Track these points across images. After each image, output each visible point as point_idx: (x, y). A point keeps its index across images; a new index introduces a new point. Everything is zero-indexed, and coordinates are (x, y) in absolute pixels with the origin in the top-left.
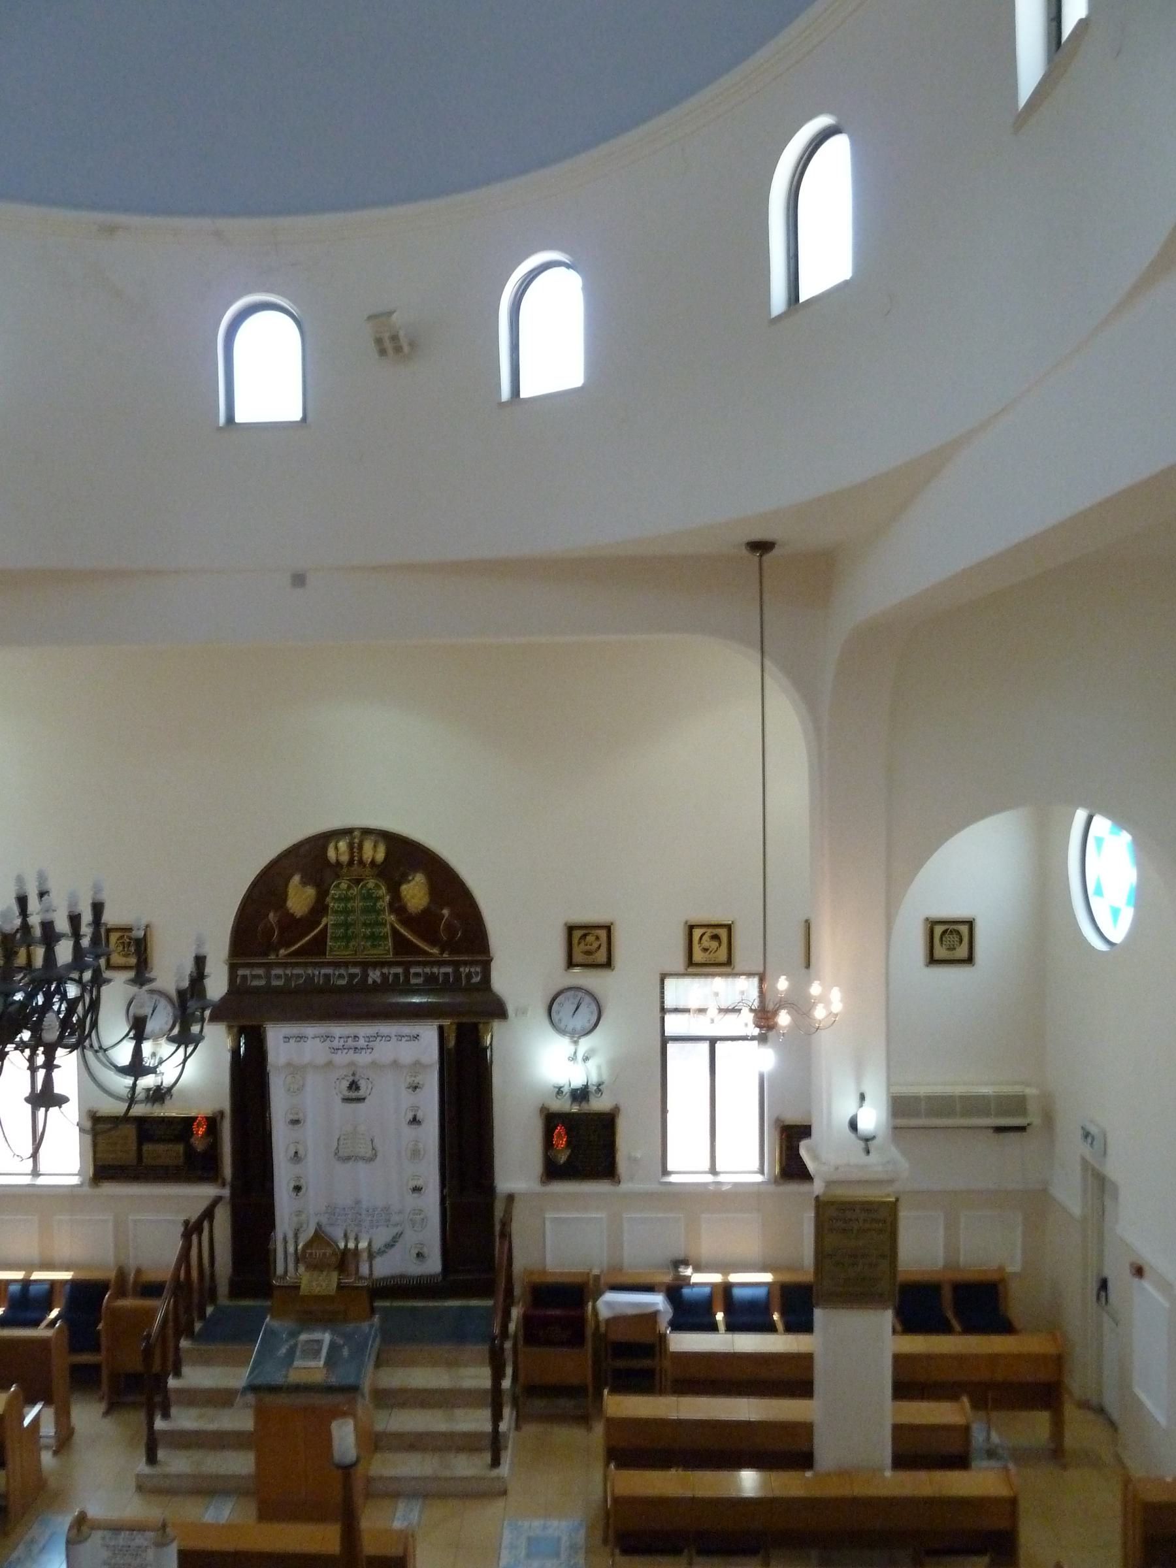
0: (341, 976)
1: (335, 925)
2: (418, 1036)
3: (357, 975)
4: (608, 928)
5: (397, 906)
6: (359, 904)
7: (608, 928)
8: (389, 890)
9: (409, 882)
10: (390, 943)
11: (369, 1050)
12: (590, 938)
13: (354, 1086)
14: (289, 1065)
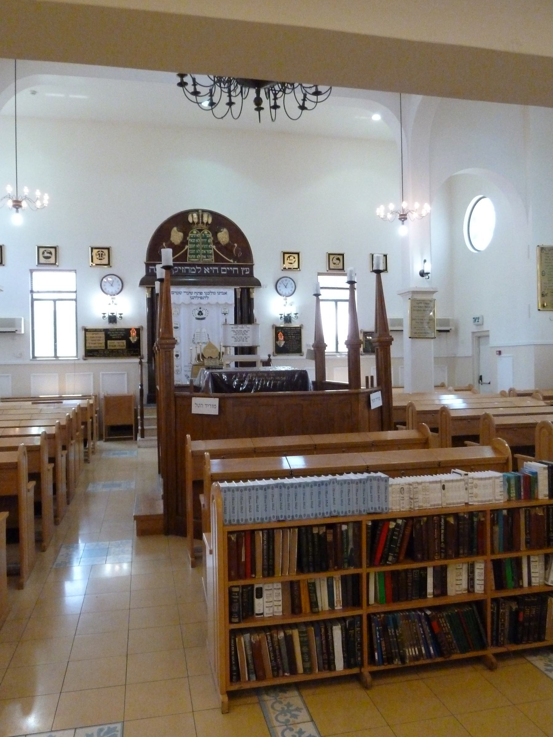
1: (190, 249)
3: (200, 269)
4: (298, 254)
5: (216, 242)
6: (200, 240)
7: (298, 254)
8: (212, 236)
9: (221, 231)
10: (213, 256)
11: (207, 298)
12: (291, 258)
13: (200, 313)
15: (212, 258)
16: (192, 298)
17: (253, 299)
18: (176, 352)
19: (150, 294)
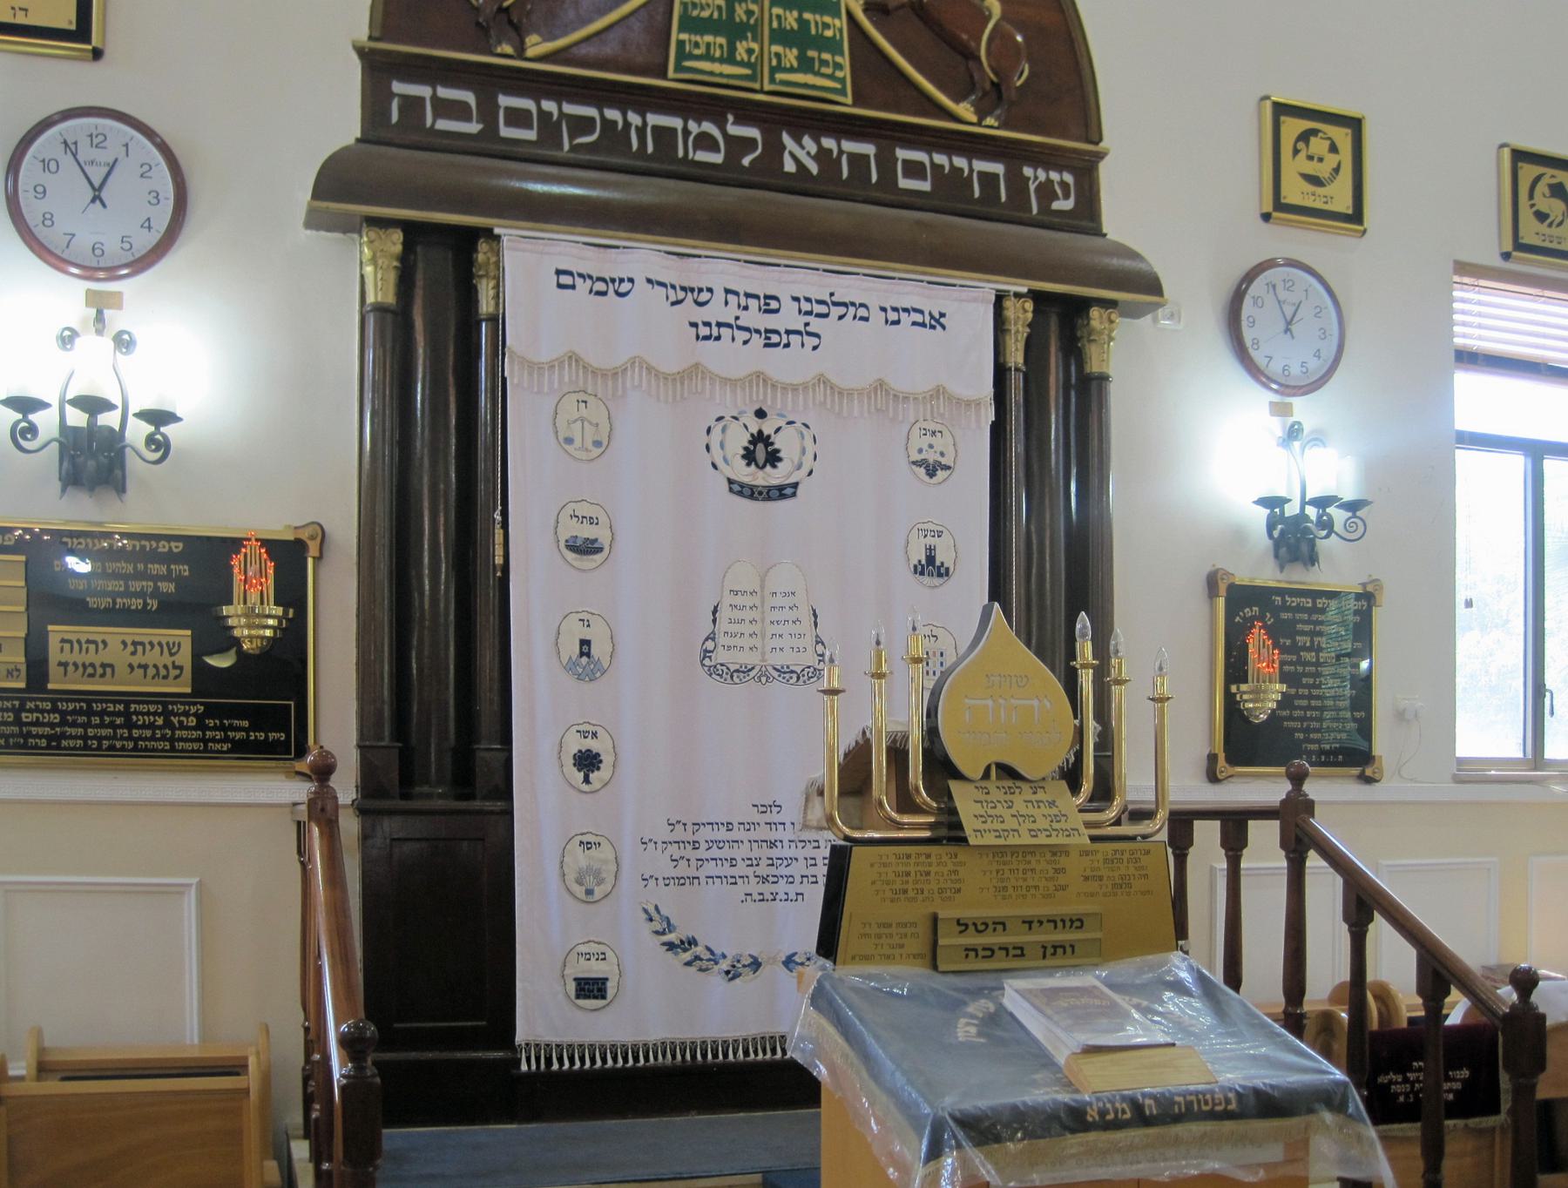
0: (705, 142)
2: (942, 315)
10: (845, 61)
13: (762, 450)
14: (574, 358)
15: (839, 74)
16: (708, 333)
17: (1103, 378)
18: (585, 734)
19: (392, 277)
